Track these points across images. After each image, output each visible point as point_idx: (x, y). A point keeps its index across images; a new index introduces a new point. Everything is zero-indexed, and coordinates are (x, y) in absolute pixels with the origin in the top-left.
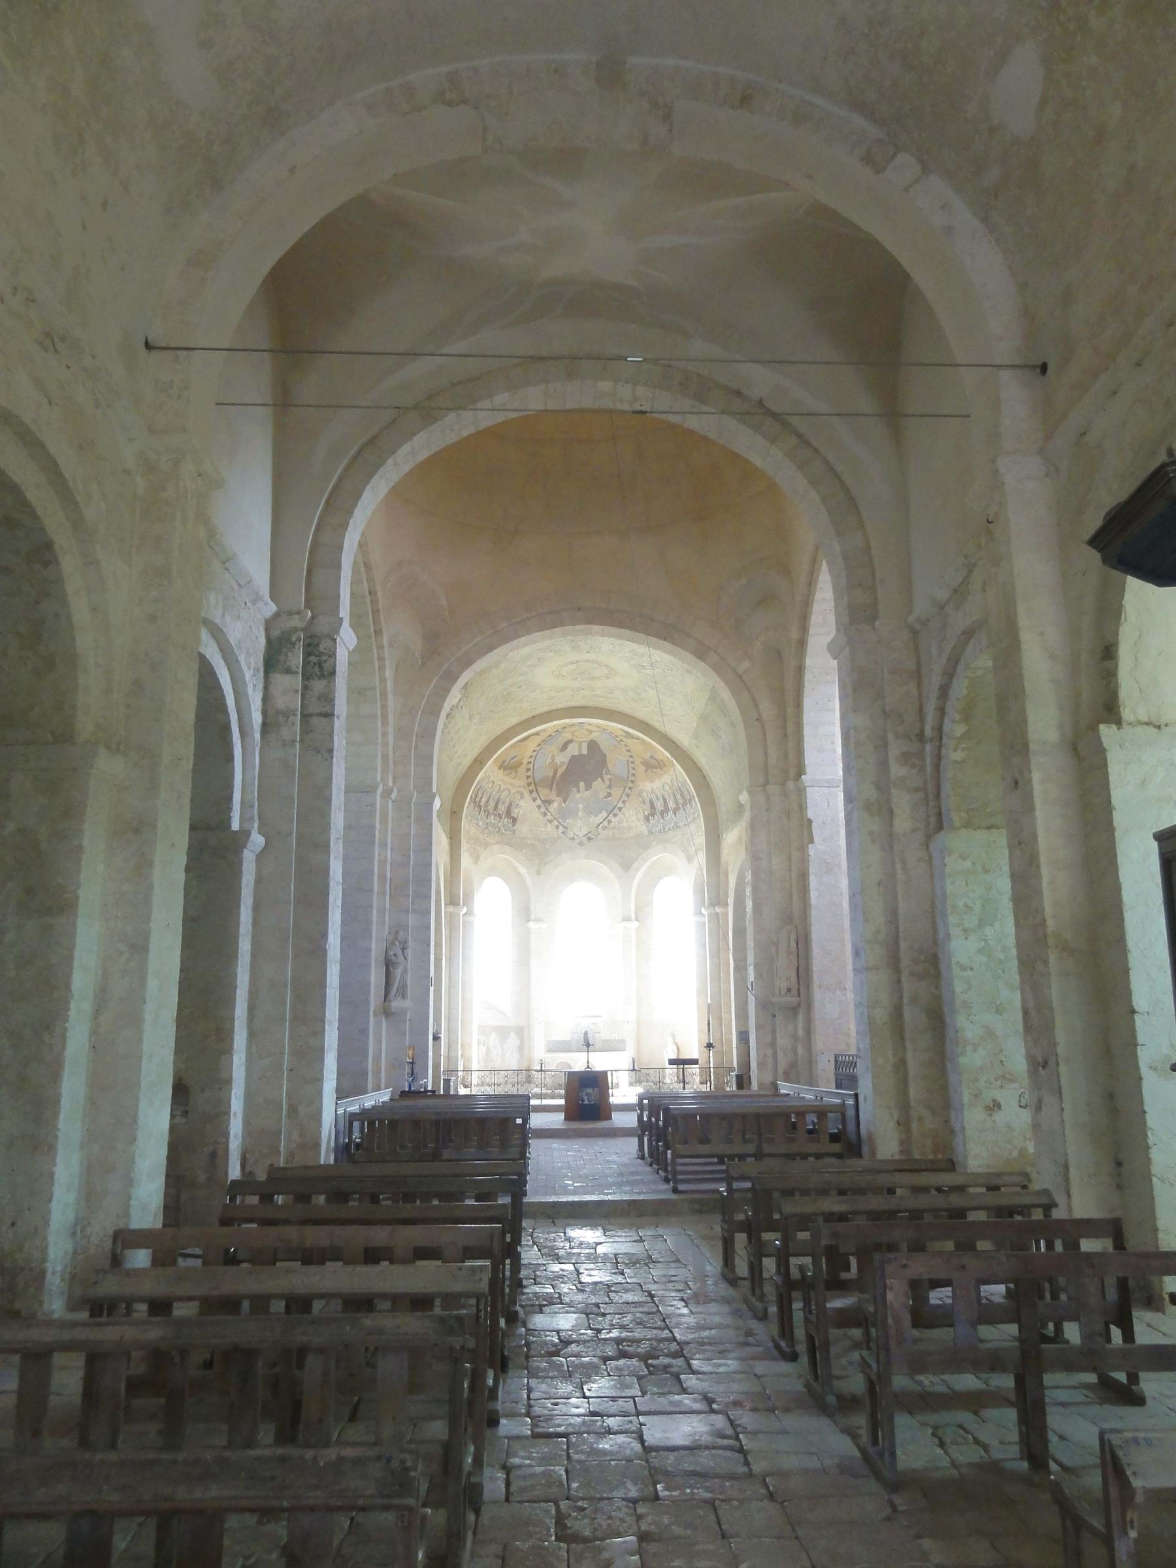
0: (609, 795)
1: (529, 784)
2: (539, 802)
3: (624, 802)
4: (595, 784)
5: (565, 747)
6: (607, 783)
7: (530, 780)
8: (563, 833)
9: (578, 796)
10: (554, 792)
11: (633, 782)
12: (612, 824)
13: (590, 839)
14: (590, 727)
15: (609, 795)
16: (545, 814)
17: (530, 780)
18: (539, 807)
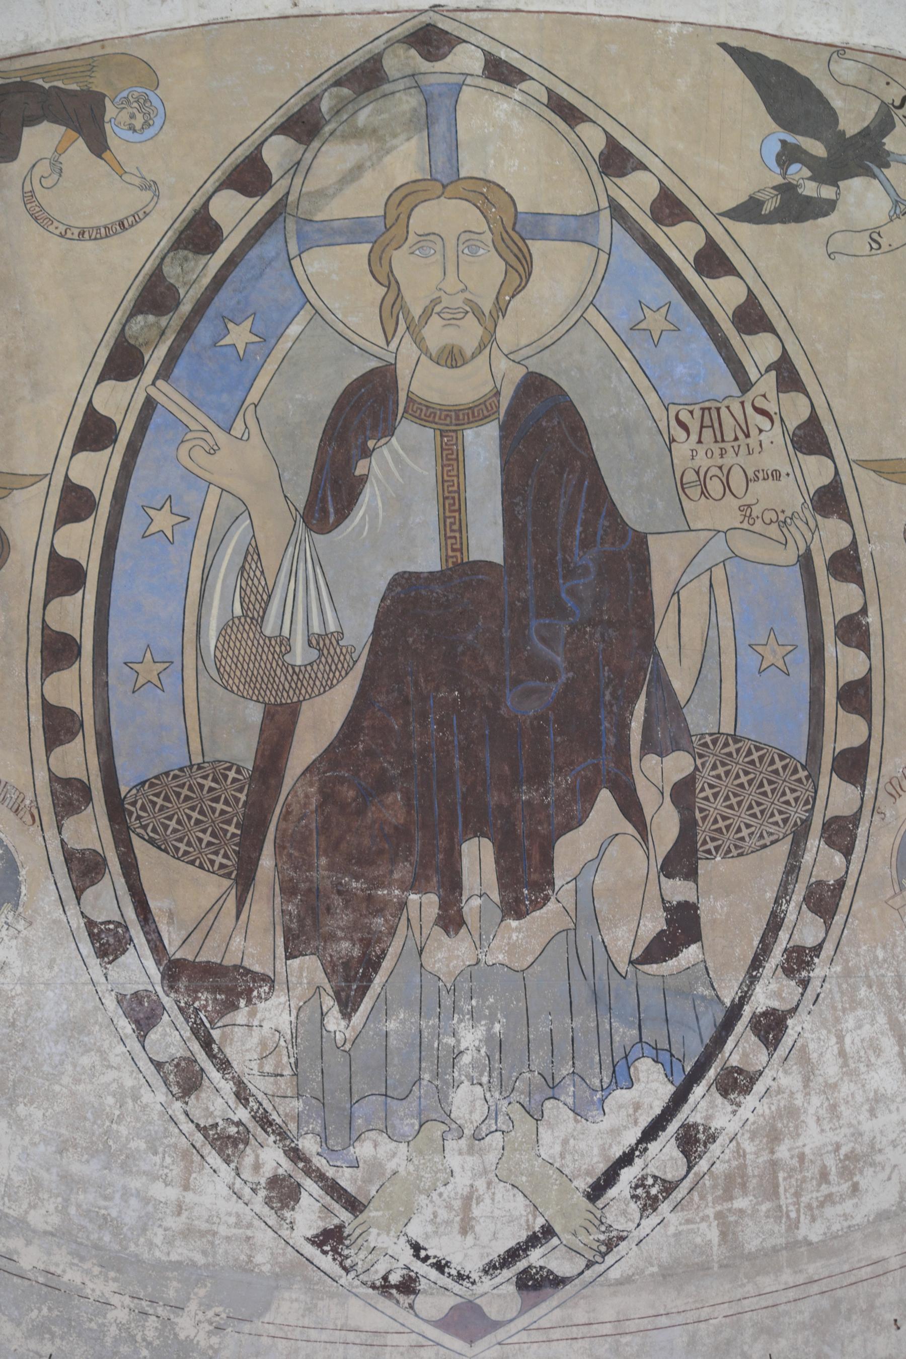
0: (683, 925)
1: (69, 796)
2: (138, 969)
3: (799, 961)
4: (570, 852)
5: (332, 495)
6: (666, 826)
7: (77, 758)
8: (330, 1239)
9: (449, 955)
10: (265, 905)
11: (853, 765)
12: (716, 1158)
13: (535, 1284)
14: (503, 140)
15: (683, 925)
16: (188, 1082)
17: (77, 758)
18: (143, 1015)
